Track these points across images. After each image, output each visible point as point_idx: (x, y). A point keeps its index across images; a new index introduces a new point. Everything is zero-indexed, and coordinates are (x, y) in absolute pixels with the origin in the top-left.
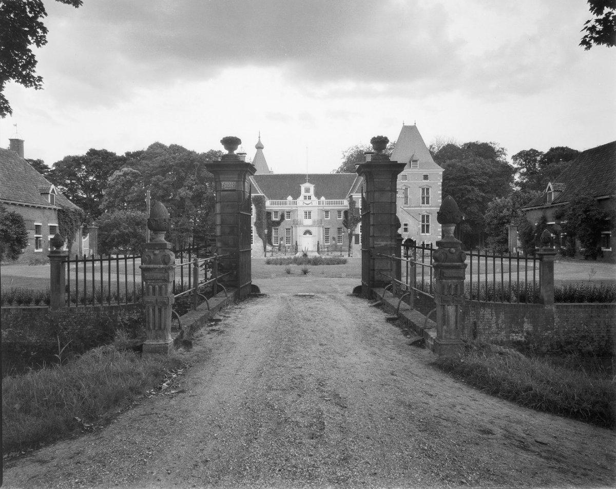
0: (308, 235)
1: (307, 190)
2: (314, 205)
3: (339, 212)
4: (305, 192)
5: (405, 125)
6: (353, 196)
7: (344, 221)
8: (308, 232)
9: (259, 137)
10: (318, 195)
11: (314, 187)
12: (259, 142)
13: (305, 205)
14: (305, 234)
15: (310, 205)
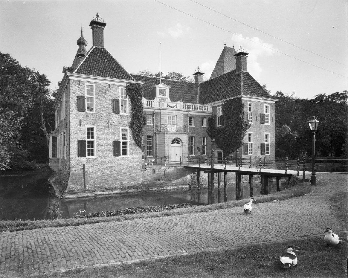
0: (176, 144)
1: (162, 92)
2: (178, 108)
3: (203, 117)
4: (160, 95)
5: (226, 46)
6: (242, 98)
7: (208, 129)
8: (176, 141)
9: (82, 32)
10: (173, 98)
11: (170, 89)
12: (82, 36)
13: (169, 108)
14: (173, 142)
15: (175, 108)
